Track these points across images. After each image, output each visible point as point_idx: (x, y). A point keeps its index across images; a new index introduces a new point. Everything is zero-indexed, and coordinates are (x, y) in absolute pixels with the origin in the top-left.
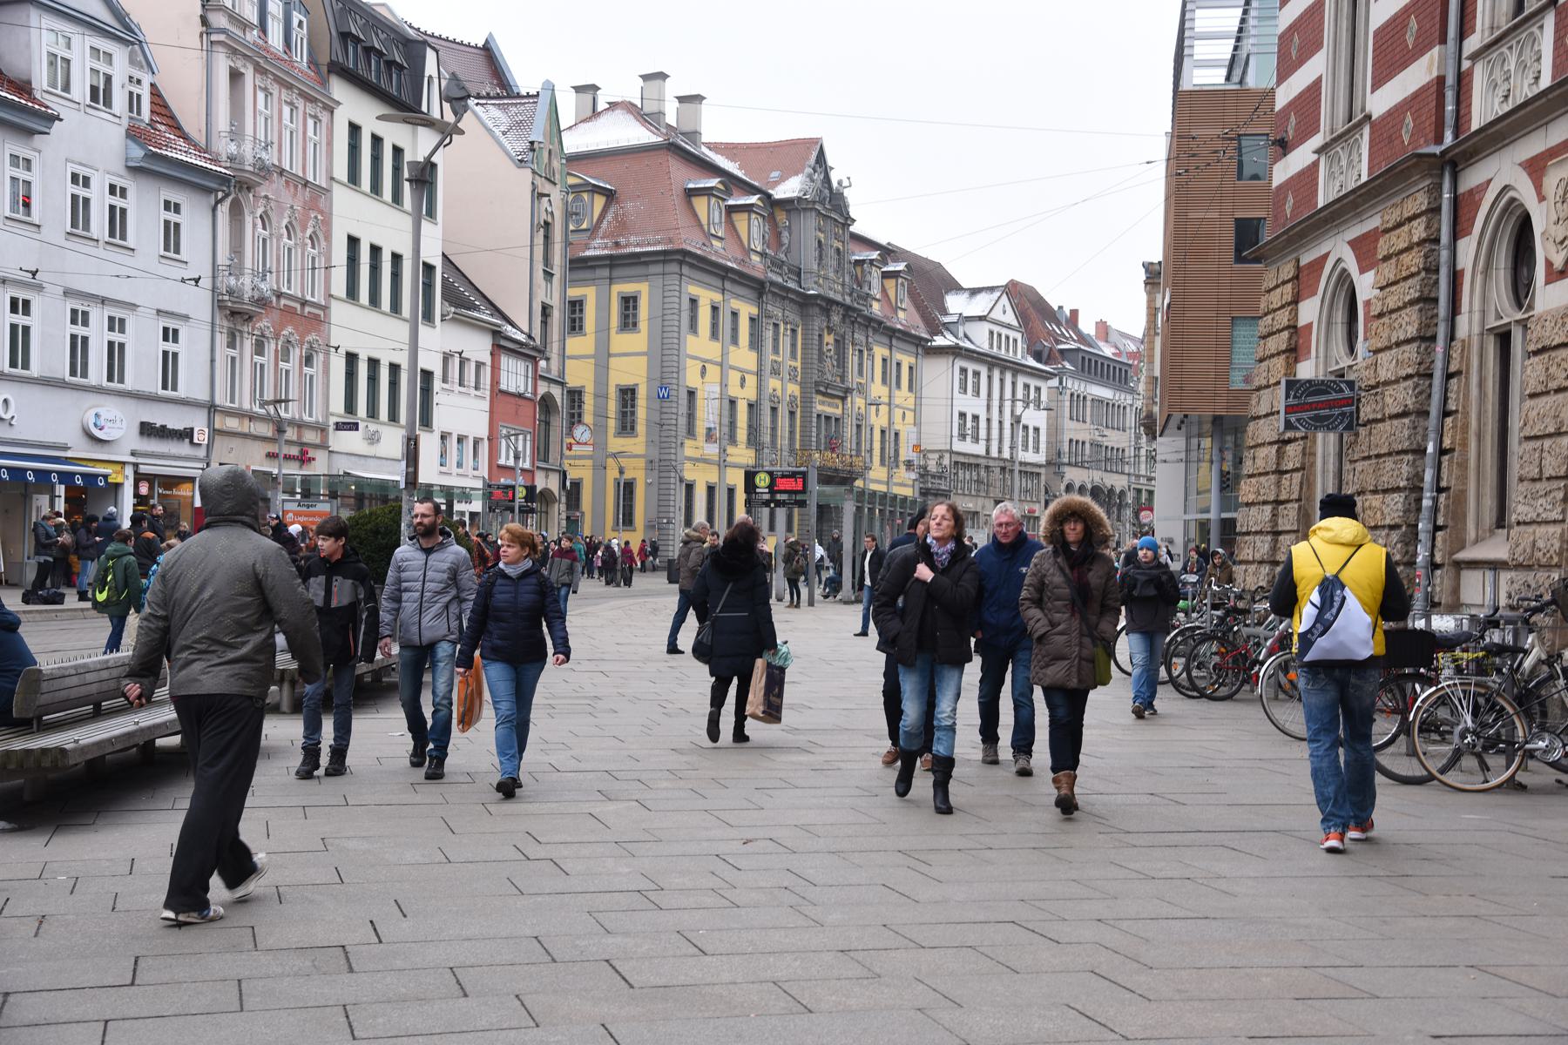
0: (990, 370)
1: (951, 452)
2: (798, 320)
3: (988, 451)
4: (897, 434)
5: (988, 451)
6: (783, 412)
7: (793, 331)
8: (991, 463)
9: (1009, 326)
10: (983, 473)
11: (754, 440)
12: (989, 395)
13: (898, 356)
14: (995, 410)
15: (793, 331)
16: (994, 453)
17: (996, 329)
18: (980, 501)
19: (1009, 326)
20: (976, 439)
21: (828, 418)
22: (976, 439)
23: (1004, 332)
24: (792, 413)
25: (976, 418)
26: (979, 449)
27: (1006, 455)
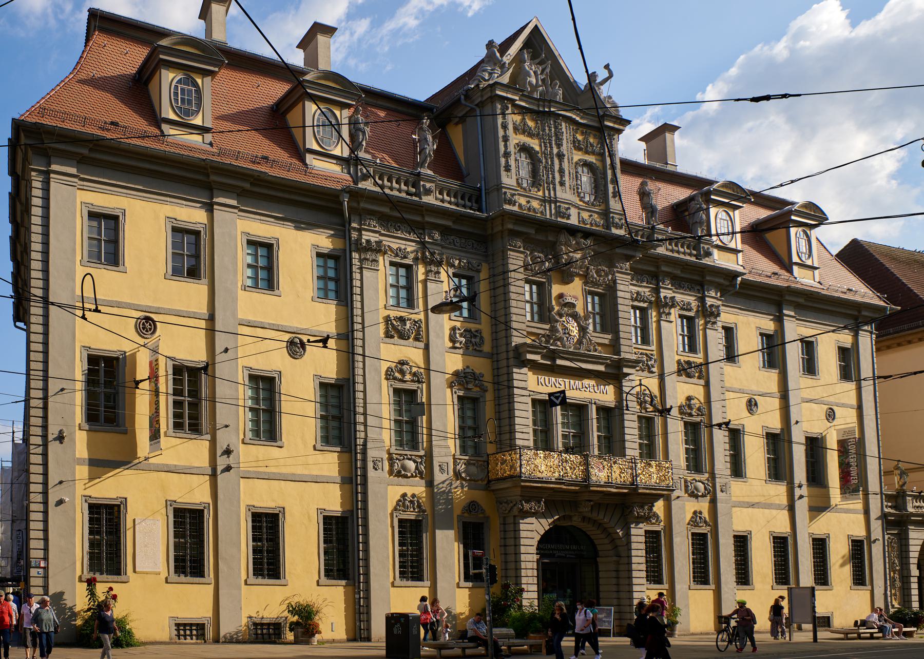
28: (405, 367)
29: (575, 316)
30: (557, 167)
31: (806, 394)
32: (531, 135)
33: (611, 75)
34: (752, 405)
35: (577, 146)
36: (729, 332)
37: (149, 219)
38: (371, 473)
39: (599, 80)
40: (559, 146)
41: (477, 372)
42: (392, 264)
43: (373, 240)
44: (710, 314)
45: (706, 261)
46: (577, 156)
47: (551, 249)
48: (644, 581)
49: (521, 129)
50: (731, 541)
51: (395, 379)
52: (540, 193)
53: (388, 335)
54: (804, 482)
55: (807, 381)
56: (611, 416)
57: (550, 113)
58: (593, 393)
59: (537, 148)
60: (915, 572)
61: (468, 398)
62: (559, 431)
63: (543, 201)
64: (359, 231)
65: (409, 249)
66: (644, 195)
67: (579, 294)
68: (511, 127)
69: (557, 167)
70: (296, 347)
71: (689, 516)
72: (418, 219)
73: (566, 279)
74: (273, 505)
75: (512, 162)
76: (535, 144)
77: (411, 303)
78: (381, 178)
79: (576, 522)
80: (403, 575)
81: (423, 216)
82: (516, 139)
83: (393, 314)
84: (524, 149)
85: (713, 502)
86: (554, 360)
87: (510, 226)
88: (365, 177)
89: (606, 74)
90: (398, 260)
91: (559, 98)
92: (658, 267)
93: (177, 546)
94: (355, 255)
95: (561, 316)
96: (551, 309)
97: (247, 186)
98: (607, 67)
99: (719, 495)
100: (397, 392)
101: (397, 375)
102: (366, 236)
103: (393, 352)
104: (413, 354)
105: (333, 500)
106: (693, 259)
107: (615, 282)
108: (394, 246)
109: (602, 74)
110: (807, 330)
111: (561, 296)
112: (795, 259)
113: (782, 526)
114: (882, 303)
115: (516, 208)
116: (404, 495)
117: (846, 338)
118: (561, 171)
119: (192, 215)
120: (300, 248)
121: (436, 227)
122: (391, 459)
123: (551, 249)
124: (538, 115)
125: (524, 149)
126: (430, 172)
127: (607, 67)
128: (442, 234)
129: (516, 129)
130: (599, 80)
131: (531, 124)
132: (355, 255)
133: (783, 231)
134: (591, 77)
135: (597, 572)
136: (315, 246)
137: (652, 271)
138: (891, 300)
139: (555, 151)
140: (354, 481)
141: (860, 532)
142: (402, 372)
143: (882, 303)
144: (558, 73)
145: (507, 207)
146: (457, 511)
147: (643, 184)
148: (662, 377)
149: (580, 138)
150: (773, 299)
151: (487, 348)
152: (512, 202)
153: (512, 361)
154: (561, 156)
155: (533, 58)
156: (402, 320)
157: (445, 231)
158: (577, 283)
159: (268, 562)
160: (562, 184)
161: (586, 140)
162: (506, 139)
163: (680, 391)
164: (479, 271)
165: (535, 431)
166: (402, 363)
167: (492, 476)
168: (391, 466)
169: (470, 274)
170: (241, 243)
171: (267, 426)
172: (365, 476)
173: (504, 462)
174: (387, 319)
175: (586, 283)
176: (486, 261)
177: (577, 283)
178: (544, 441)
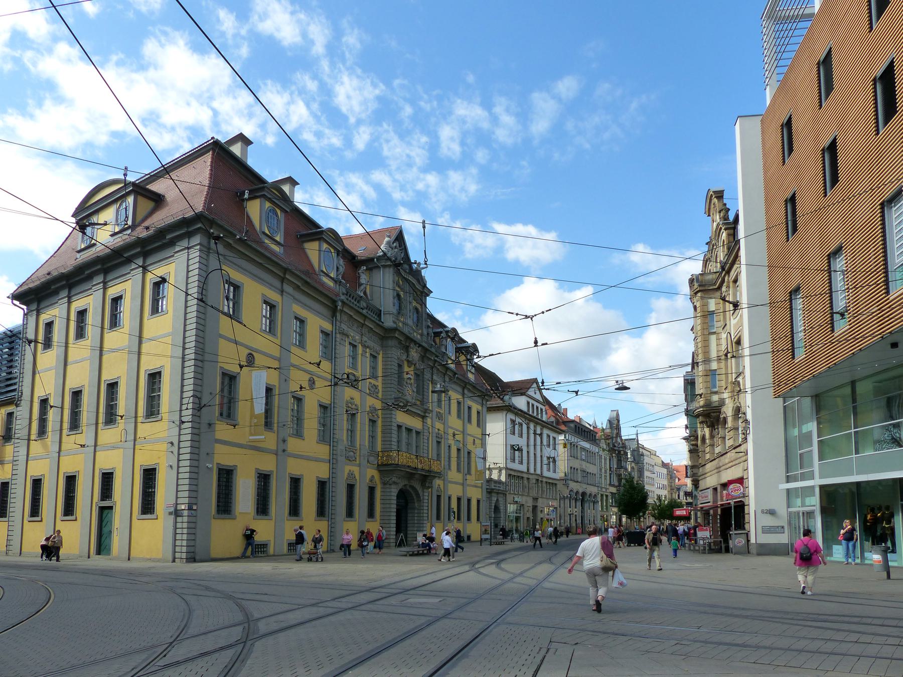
0: (528, 424)
1: (507, 469)
2: (378, 348)
3: (528, 469)
4: (469, 453)
5: (528, 469)
6: (362, 421)
7: (374, 357)
8: (530, 477)
9: (538, 401)
10: (526, 482)
11: (326, 434)
12: (528, 438)
13: (469, 402)
14: (532, 448)
15: (374, 357)
16: (532, 471)
17: (531, 401)
18: (524, 498)
19: (538, 401)
20: (521, 463)
21: (409, 430)
22: (521, 463)
23: (536, 404)
24: (373, 422)
26: (523, 468)
27: (539, 472)
42: (350, 343)
46: (414, 304)
47: (407, 349)
55: (469, 425)
63: (404, 323)
76: (402, 294)
94: (338, 336)
102: (344, 326)
105: (323, 472)
113: (460, 494)
117: (480, 408)
123: (407, 349)
132: (338, 336)
140: (333, 461)
150: (464, 385)
151: (380, 395)
159: (295, 510)
163: (439, 425)
166: (352, 399)
170: (293, 318)
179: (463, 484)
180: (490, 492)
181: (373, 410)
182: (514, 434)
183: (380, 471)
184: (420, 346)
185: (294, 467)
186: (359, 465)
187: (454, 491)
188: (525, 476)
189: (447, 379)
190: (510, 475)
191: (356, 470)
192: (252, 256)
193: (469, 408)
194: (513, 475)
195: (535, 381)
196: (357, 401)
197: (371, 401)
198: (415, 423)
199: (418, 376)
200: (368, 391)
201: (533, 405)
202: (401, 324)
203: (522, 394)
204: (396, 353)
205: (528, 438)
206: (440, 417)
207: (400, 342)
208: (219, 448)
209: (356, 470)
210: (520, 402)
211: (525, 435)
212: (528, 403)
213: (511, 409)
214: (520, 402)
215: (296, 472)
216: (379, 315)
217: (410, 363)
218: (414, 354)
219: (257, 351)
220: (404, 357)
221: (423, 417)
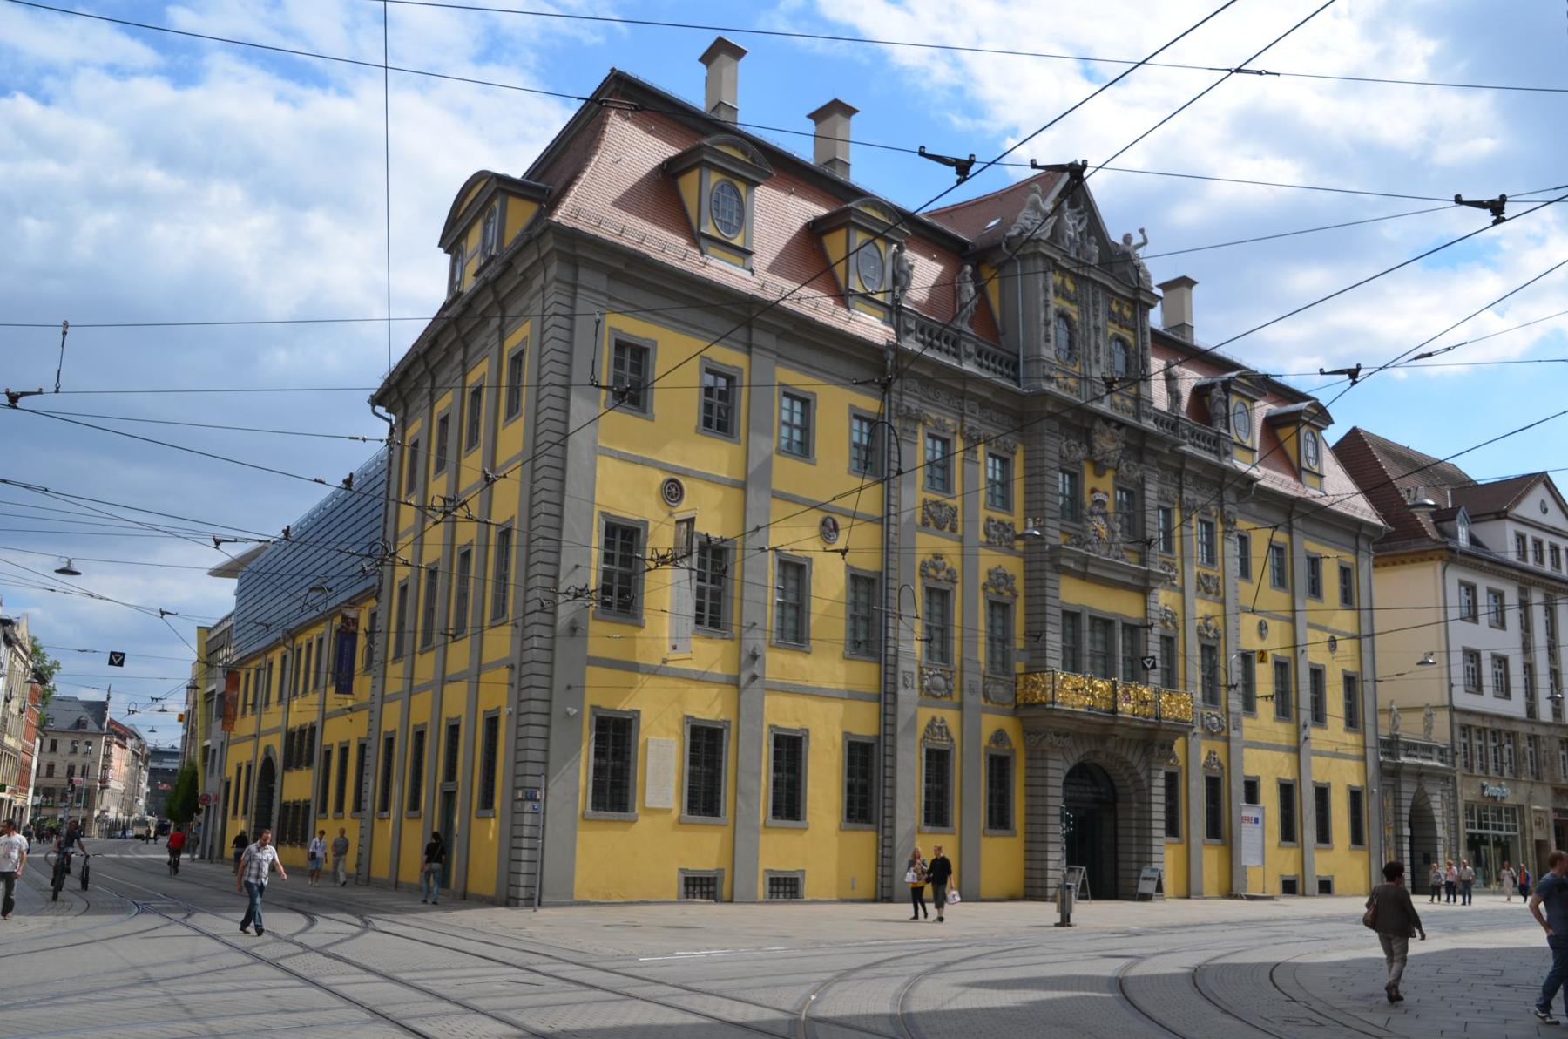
0: (1523, 591)
1: (1452, 709)
3: (1531, 710)
5: (1531, 710)
8: (1539, 731)
10: (1524, 744)
12: (1526, 627)
17: (1530, 534)
20: (1504, 691)
21: (1104, 624)
23: (1547, 539)
25: (1501, 661)
26: (1515, 707)
28: (938, 562)
29: (1105, 515)
30: (1092, 342)
31: (1313, 618)
32: (1072, 302)
33: (1145, 243)
34: (1263, 628)
35: (1112, 317)
36: (1244, 541)
37: (680, 361)
38: (901, 692)
39: (1134, 243)
40: (1096, 316)
41: (1009, 573)
43: (914, 407)
44: (1228, 523)
45: (1226, 463)
46: (1113, 329)
47: (1086, 436)
48: (1162, 833)
49: (1061, 292)
50: (1243, 788)
51: (928, 576)
52: (1077, 369)
53: (925, 524)
54: (1309, 722)
55: (1312, 604)
56: (1134, 631)
57: (1088, 279)
58: (1124, 606)
59: (1075, 316)
60: (1407, 831)
61: (999, 604)
62: (1087, 646)
64: (901, 394)
65: (949, 421)
66: (1170, 379)
67: (1110, 489)
68: (1051, 290)
69: (1092, 342)
70: (829, 529)
71: (1204, 755)
72: (959, 386)
73: (1099, 470)
74: (795, 725)
75: (1052, 332)
76: (1073, 311)
77: (946, 487)
78: (922, 332)
79: (1101, 760)
80: (928, 821)
81: (964, 385)
82: (1056, 303)
83: (931, 497)
84: (1063, 315)
85: (1227, 740)
86: (1086, 566)
87: (1050, 408)
88: (908, 332)
89: (1141, 240)
90: (937, 433)
91: (1095, 261)
92: (1182, 464)
93: (692, 775)
95: (1092, 514)
96: (1082, 506)
97: (789, 327)
98: (1142, 231)
99: (1233, 734)
100: (930, 591)
101: (932, 572)
103: (927, 544)
104: (948, 547)
106: (1212, 458)
107: (1143, 479)
108: (935, 416)
109: (1137, 239)
110: (1314, 548)
111: (1093, 491)
112: (1304, 465)
113: (1288, 776)
114: (1379, 523)
115: (1052, 387)
116: (934, 719)
117: (1349, 558)
118: (1097, 347)
119: (729, 357)
120: (839, 408)
121: (974, 397)
122: (921, 673)
123: (1086, 436)
124: (1077, 279)
125: (1063, 315)
126: (970, 330)
127: (1142, 231)
128: (981, 406)
129: (1056, 293)
130: (1134, 243)
131: (1070, 287)
133: (1292, 429)
134: (1127, 238)
135: (1116, 820)
136: (852, 407)
137: (1179, 469)
138: (1386, 518)
139: (1092, 322)
140: (886, 697)
141: (1356, 782)
142: (934, 567)
143: (1379, 523)
144: (1094, 225)
145: (1046, 386)
146: (985, 741)
147: (1169, 366)
148: (1182, 591)
149: (1115, 308)
152: (1049, 379)
153: (1048, 566)
154: (1097, 329)
155: (1073, 205)
156: (937, 504)
157: (984, 404)
158: (1110, 474)
160: (1098, 361)
161: (1121, 311)
162: (1047, 306)
163: (1202, 608)
164: (1014, 453)
165: (1064, 648)
166: (938, 557)
167: (1020, 700)
168: (921, 682)
169: (1006, 455)
171: (795, 629)
172: (895, 695)
173: (1035, 684)
174: (925, 504)
175: (1116, 478)
176: (1022, 442)
177: (1110, 474)
178: (1073, 663)
179: (1297, 750)
180: (1391, 775)
181: (999, 579)
182: (1474, 617)
183: (1021, 719)
184: (1121, 425)
185: (782, 713)
186: (960, 707)
187: (1268, 767)
188: (1523, 729)
189: (1230, 496)
190: (1465, 729)
191: (950, 717)
192: (659, 282)
193: (1314, 562)
194: (1470, 726)
195: (1543, 479)
196: (953, 560)
197: (989, 560)
198: (1124, 606)
199: (1133, 494)
200: (983, 538)
201: (1538, 544)
202: (1072, 382)
203: (1501, 515)
204: (1054, 447)
205: (1526, 627)
206: (1207, 587)
207: (1065, 424)
208: (595, 675)
209: (950, 717)
210: (1503, 539)
211: (1513, 617)
212: (1521, 538)
213: (1479, 559)
214: (1503, 539)
215: (790, 723)
216: (1016, 367)
217: (1099, 470)
218: (1108, 444)
219: (687, 473)
220: (1081, 454)
221: (1145, 591)
